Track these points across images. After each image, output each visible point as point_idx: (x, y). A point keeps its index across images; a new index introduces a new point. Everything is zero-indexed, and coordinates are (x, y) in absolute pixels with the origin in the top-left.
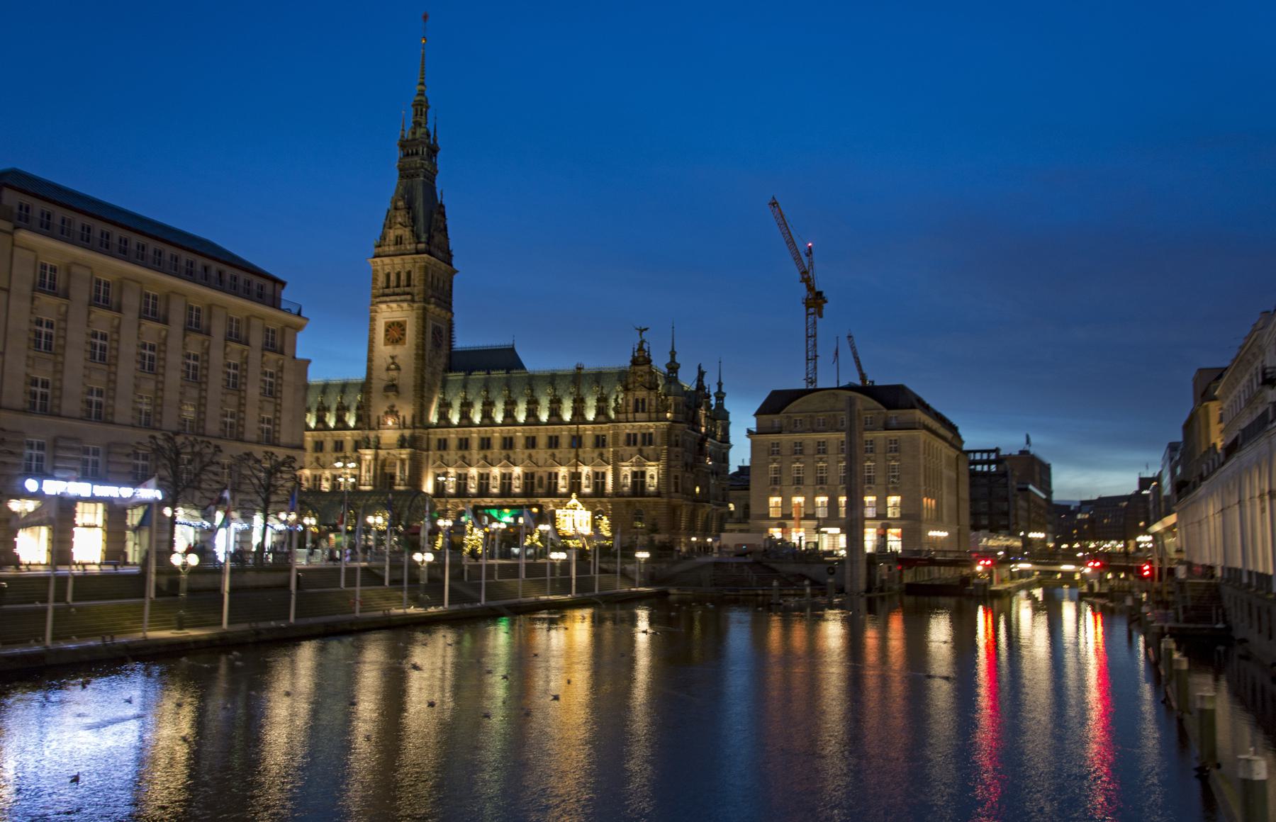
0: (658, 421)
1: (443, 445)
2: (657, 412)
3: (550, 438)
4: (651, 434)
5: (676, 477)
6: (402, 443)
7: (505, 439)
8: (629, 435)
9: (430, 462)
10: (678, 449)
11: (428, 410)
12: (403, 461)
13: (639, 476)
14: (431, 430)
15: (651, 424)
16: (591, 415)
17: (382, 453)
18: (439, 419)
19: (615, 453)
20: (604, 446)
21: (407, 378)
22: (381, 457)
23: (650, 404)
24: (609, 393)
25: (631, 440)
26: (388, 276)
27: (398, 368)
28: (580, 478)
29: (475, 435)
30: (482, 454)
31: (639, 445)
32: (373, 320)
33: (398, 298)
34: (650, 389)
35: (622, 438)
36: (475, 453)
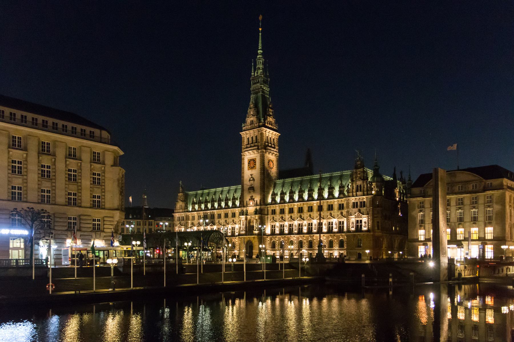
1: (274, 212)
2: (367, 190)
4: (364, 202)
5: (378, 222)
6: (256, 212)
7: (299, 208)
8: (354, 203)
10: (379, 209)
11: (267, 197)
13: (359, 223)
15: (364, 197)
16: (336, 194)
17: (249, 217)
18: (272, 201)
19: (348, 212)
20: (343, 209)
21: (257, 184)
23: (364, 187)
24: (346, 184)
25: (355, 205)
26: (248, 139)
27: (254, 180)
28: (332, 224)
29: (296, 206)
31: (359, 208)
33: (252, 148)
35: (351, 205)
36: (287, 216)
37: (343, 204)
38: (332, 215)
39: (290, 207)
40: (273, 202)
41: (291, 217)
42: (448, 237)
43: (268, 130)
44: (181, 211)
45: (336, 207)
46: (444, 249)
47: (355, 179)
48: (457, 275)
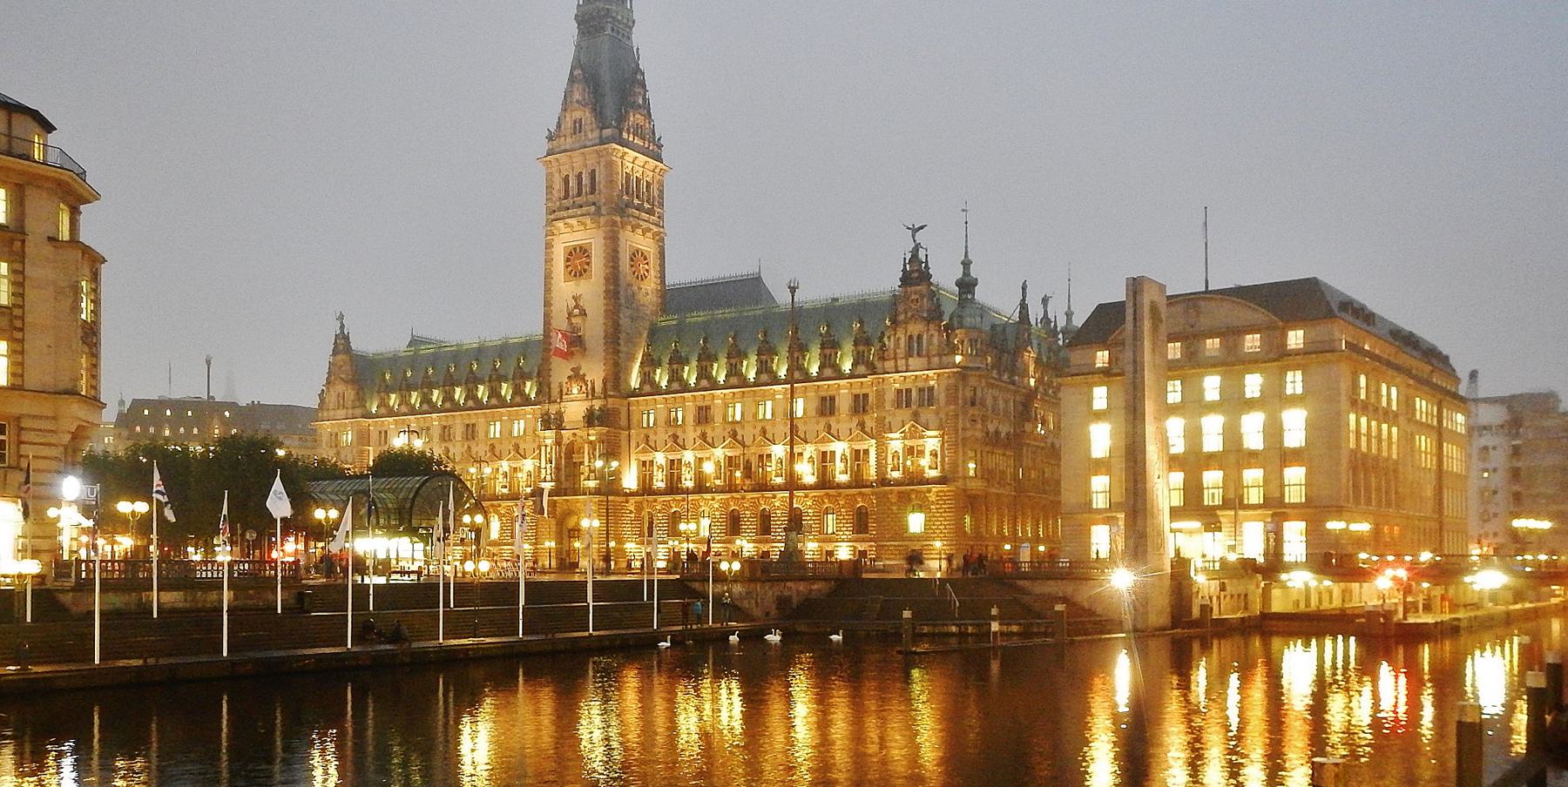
3: (823, 399)
4: (931, 389)
6: (590, 419)
8: (899, 391)
9: (633, 444)
12: (591, 442)
15: (931, 373)
19: (880, 421)
21: (594, 328)
22: (565, 441)
23: (930, 343)
25: (903, 399)
26: (566, 180)
27: (583, 313)
28: (833, 460)
31: (914, 407)
32: (549, 246)
34: (928, 321)
35: (890, 396)
37: (866, 396)
39: (700, 404)
40: (647, 388)
41: (704, 436)
42: (1177, 500)
44: (341, 413)
45: (844, 403)
46: (1160, 534)
47: (902, 317)
48: (1196, 612)
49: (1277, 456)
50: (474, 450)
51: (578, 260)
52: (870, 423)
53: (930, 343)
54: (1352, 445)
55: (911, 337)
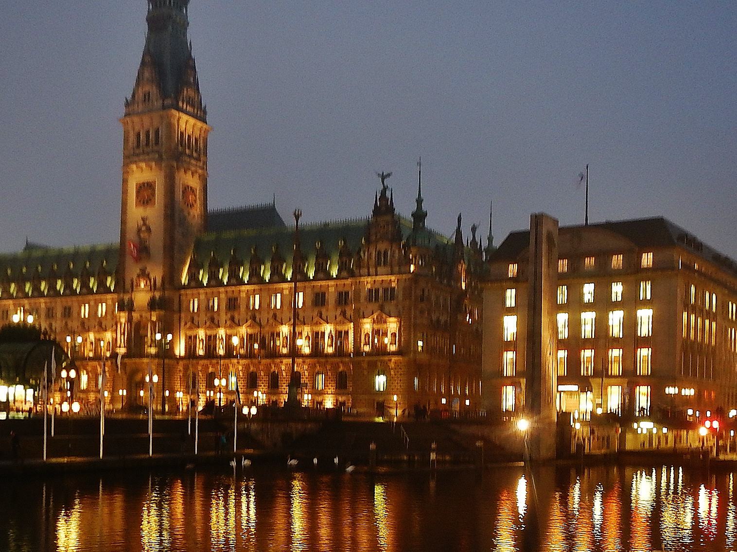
0: (400, 273)
3: (317, 295)
6: (153, 305)
9: (183, 324)
12: (153, 322)
14: (183, 292)
15: (393, 278)
17: (136, 315)
21: (156, 241)
23: (393, 256)
25: (373, 296)
26: (138, 135)
27: (149, 230)
30: (229, 315)
32: (125, 181)
35: (364, 294)
38: (324, 316)
42: (562, 371)
43: (185, 117)
46: (550, 394)
47: (373, 238)
48: (573, 448)
49: (631, 340)
50: (70, 324)
51: (145, 192)
52: (349, 313)
53: (393, 256)
54: (684, 334)
55: (379, 253)
